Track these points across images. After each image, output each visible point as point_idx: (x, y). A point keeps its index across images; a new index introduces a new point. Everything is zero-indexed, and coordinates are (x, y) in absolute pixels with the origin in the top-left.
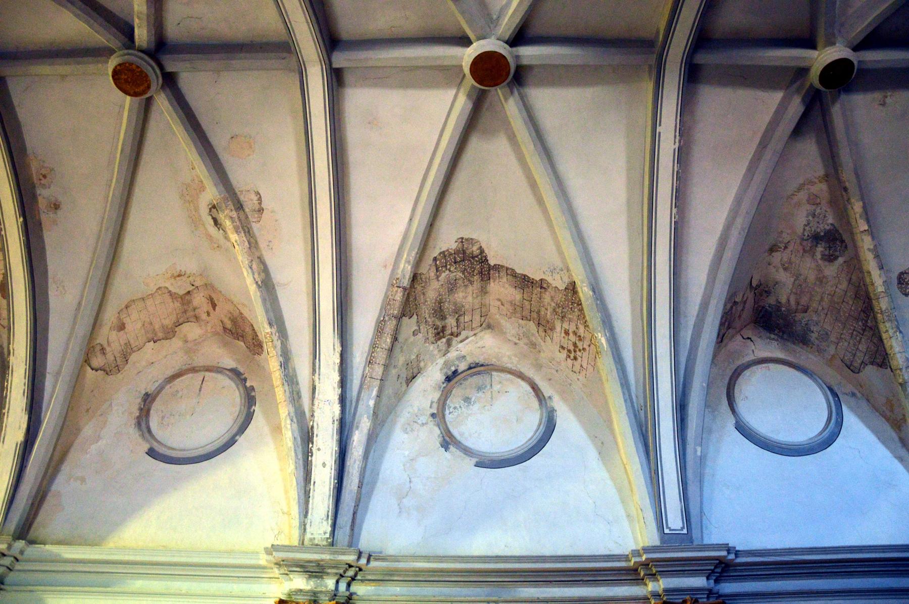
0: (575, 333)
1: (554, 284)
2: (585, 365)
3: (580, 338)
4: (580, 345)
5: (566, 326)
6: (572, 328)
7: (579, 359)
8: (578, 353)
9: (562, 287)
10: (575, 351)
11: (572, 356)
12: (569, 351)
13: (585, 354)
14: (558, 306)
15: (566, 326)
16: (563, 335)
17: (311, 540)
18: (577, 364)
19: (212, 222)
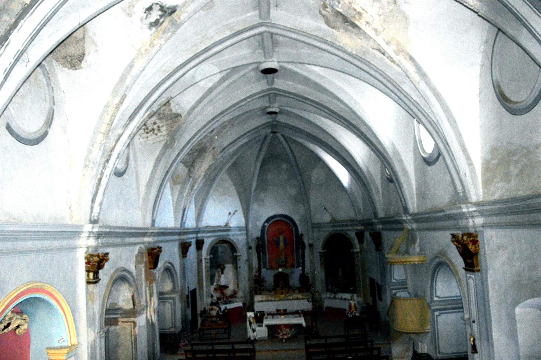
0: (159, 127)
1: (172, 108)
2: (149, 138)
3: (159, 130)
4: (156, 131)
5: (158, 121)
6: (161, 125)
7: (149, 135)
8: (151, 133)
9: (174, 111)
10: (151, 131)
11: (146, 131)
12: (147, 129)
13: (154, 136)
14: (163, 114)
15: (158, 121)
16: (152, 122)
17: (94, 216)
18: (146, 135)
19: (148, 6)
